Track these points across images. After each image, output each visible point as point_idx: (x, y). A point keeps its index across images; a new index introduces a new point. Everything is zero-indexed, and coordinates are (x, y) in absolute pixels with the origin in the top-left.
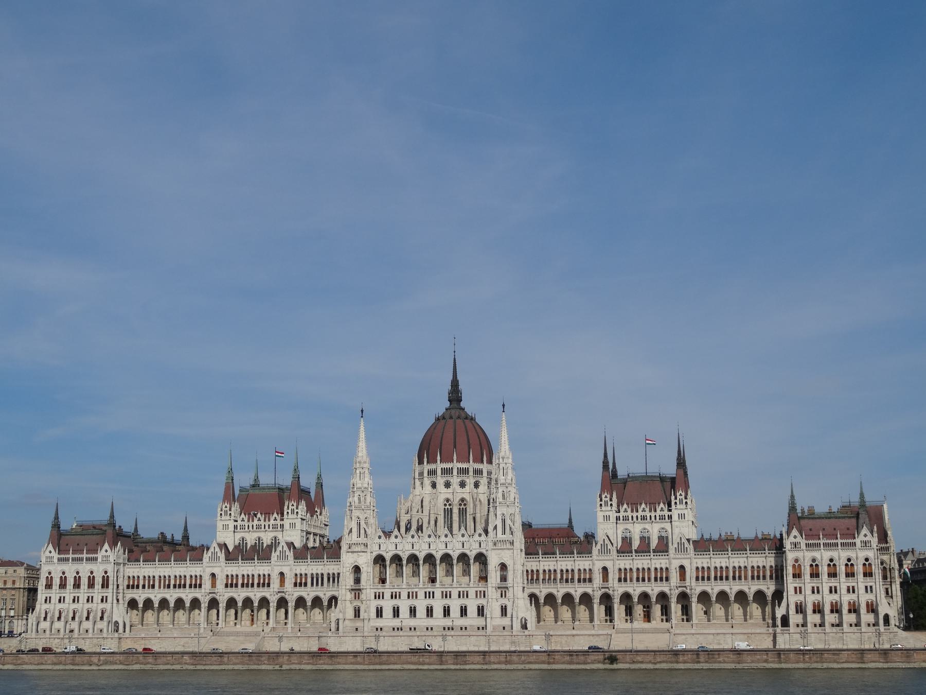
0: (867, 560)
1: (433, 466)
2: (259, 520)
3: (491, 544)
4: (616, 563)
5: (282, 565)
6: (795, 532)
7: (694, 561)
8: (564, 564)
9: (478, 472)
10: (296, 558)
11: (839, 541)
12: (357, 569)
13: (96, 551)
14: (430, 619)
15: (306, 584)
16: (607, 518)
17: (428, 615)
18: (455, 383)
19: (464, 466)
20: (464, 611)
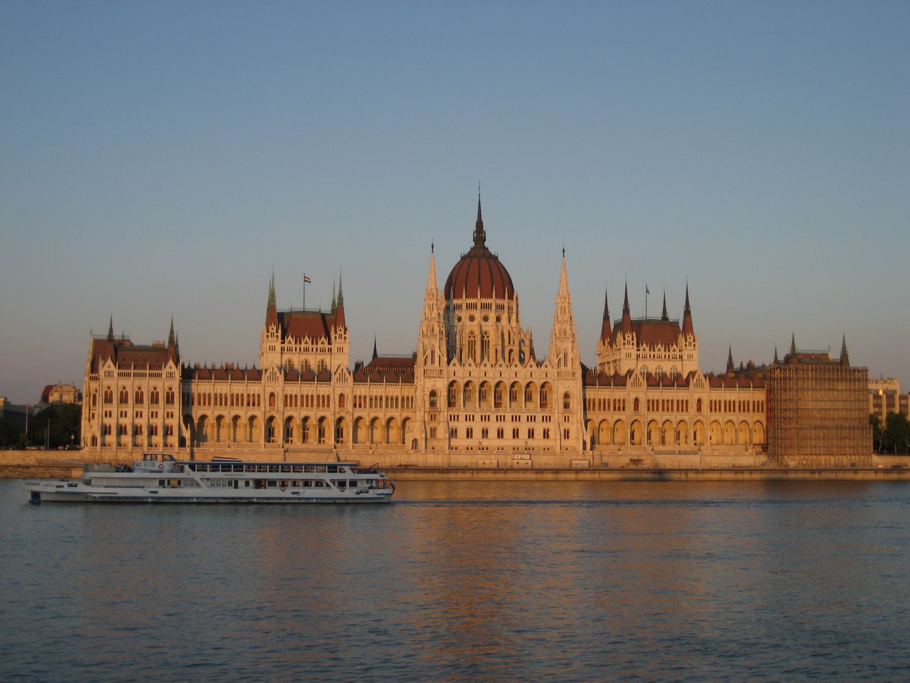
1: (473, 301)
2: (306, 343)
4: (645, 394)
8: (602, 393)
9: (510, 308)
10: (355, 381)
12: (433, 394)
14: (501, 440)
17: (498, 437)
18: (480, 224)
19: (500, 302)
20: (531, 434)
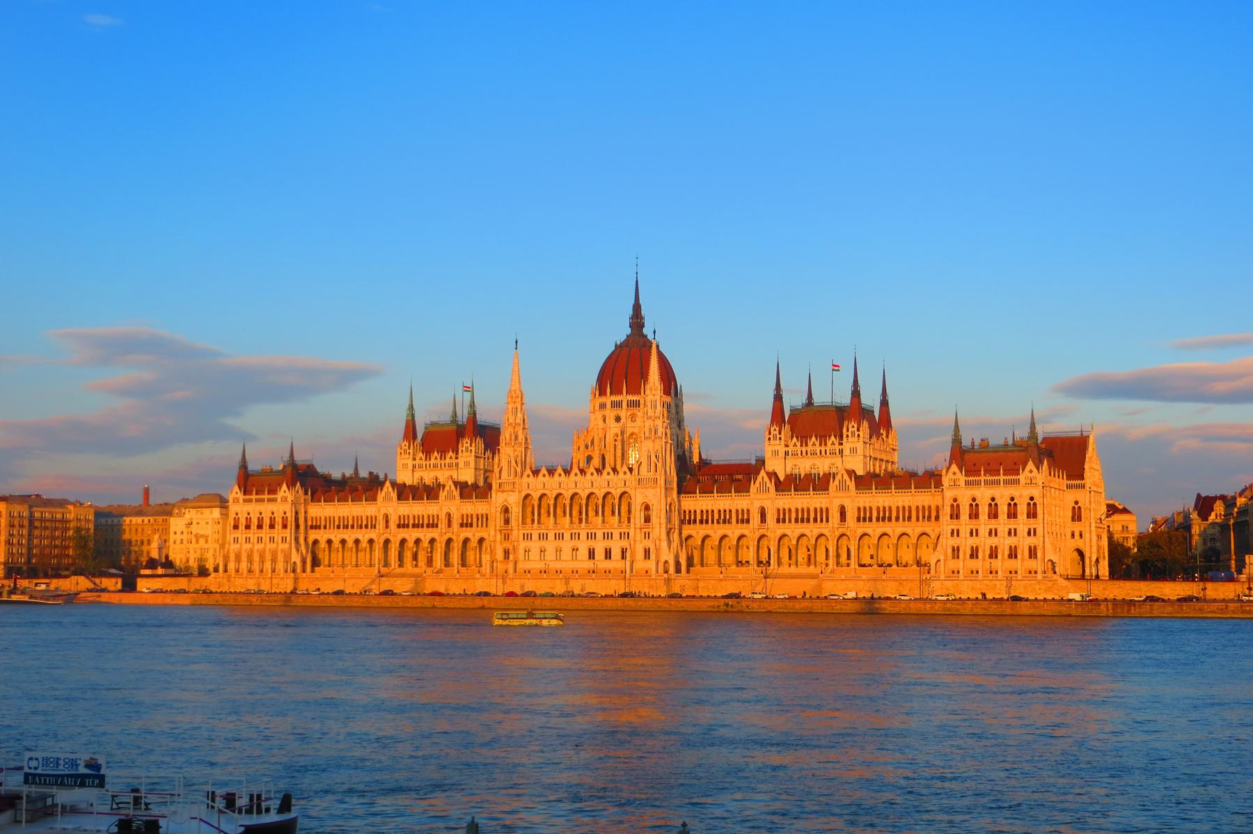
0: (1032, 499)
1: (603, 399)
3: (635, 483)
5: (450, 505)
6: (954, 468)
7: (855, 500)
10: (462, 497)
11: (1002, 478)
13: (273, 491)
15: (471, 525)
16: (776, 453)
18: (637, 307)
19: (635, 398)
20: (608, 554)
